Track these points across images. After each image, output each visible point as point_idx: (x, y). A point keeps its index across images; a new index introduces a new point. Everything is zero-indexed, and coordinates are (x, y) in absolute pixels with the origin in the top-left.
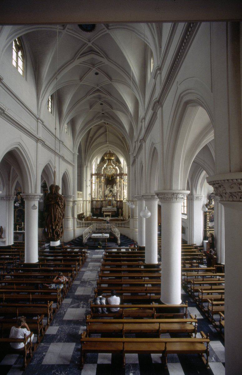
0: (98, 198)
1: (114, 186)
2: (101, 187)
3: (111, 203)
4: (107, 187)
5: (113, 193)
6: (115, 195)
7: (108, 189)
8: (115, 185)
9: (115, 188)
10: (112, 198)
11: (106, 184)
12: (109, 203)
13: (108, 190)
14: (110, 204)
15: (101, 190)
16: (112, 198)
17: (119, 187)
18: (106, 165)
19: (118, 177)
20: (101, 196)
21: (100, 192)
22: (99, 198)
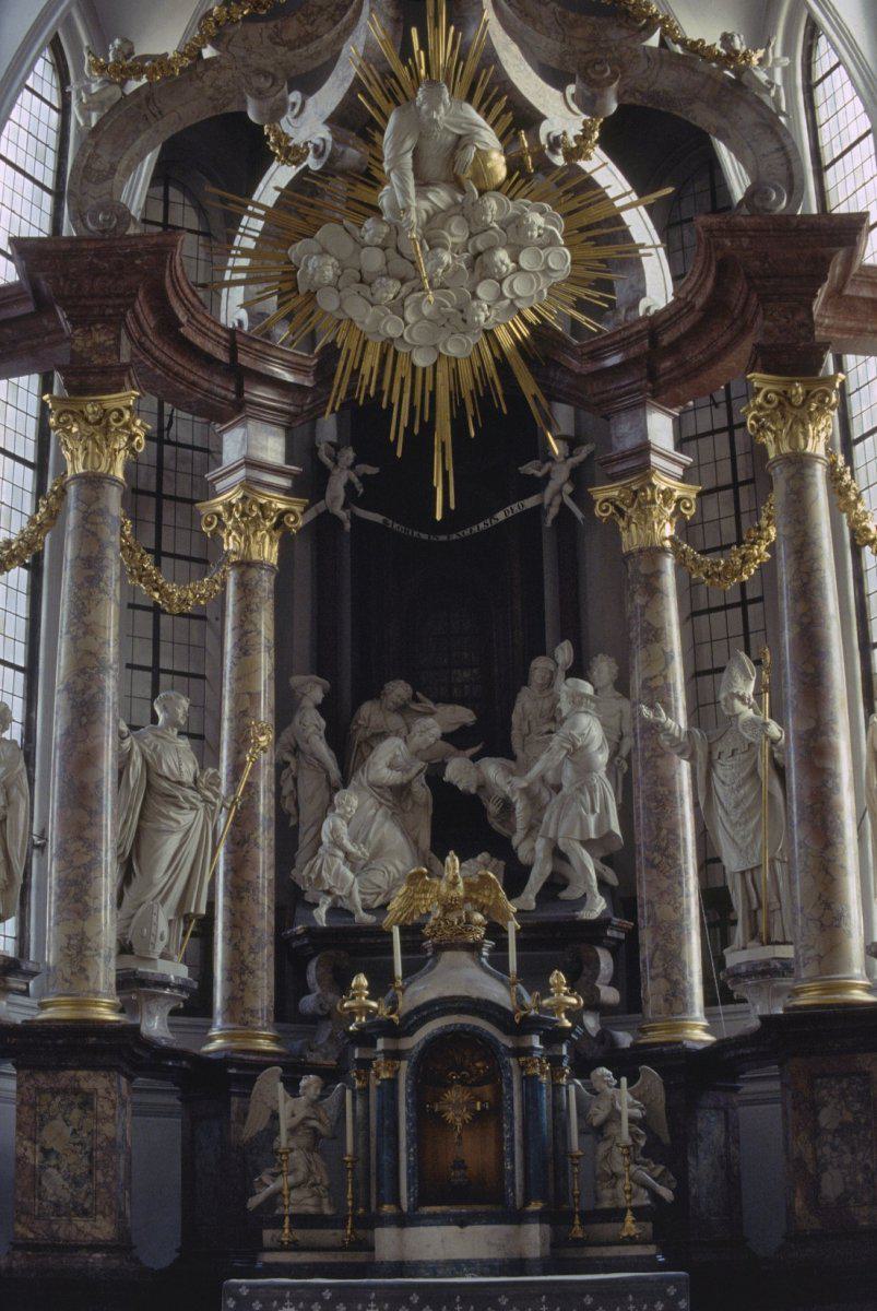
0: (78, 950)
1: (526, 703)
2: (199, 680)
3: (492, 1115)
4: (348, 747)
5: (515, 879)
6: (598, 906)
7: (387, 761)
8: (579, 669)
9: (591, 730)
10: (534, 977)
11: (323, 665)
12: (428, 1121)
13: (398, 795)
14: (472, 1151)
15: (180, 761)
16: (534, 977)
17: (703, 674)
18: (330, 96)
19: (660, 427)
20: (207, 923)
21: (154, 795)
22: (132, 985)
